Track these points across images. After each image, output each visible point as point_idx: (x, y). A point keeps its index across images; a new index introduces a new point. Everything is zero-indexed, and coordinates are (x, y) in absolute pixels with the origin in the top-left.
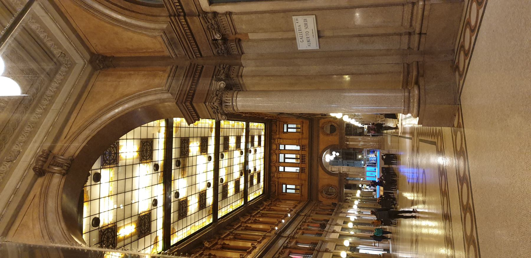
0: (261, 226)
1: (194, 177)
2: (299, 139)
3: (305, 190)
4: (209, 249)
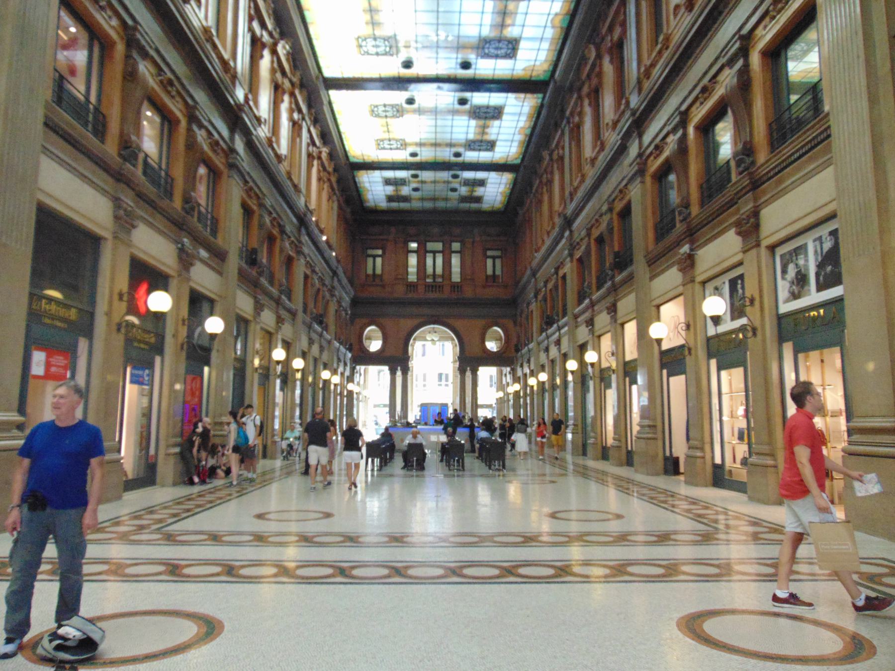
2: (473, 280)
4: (274, 52)
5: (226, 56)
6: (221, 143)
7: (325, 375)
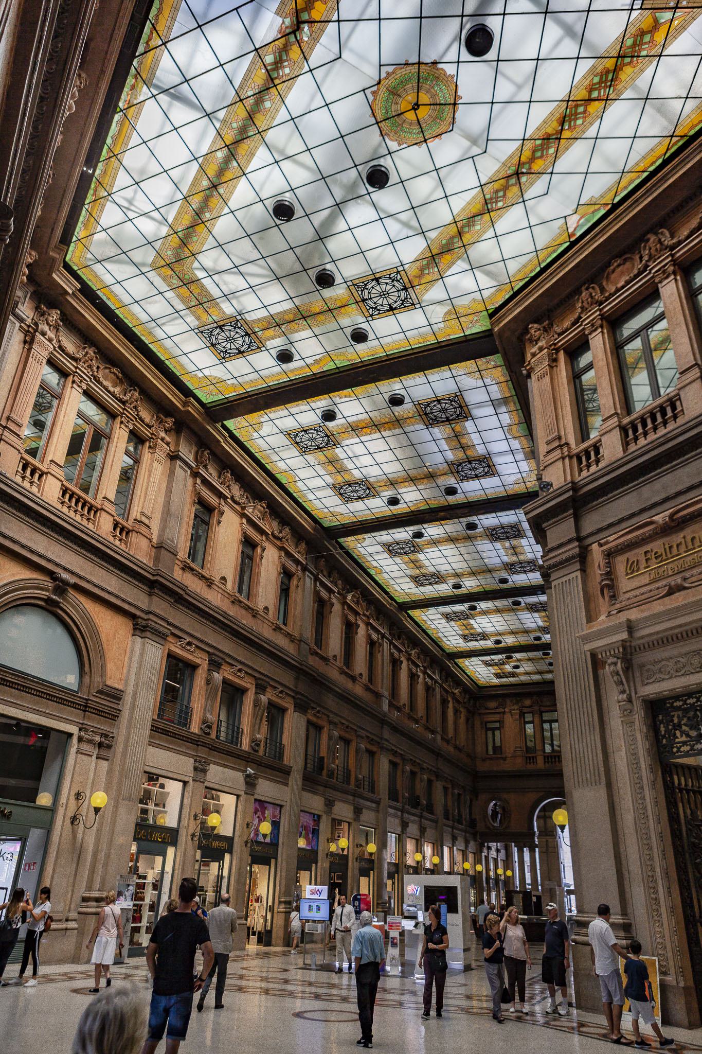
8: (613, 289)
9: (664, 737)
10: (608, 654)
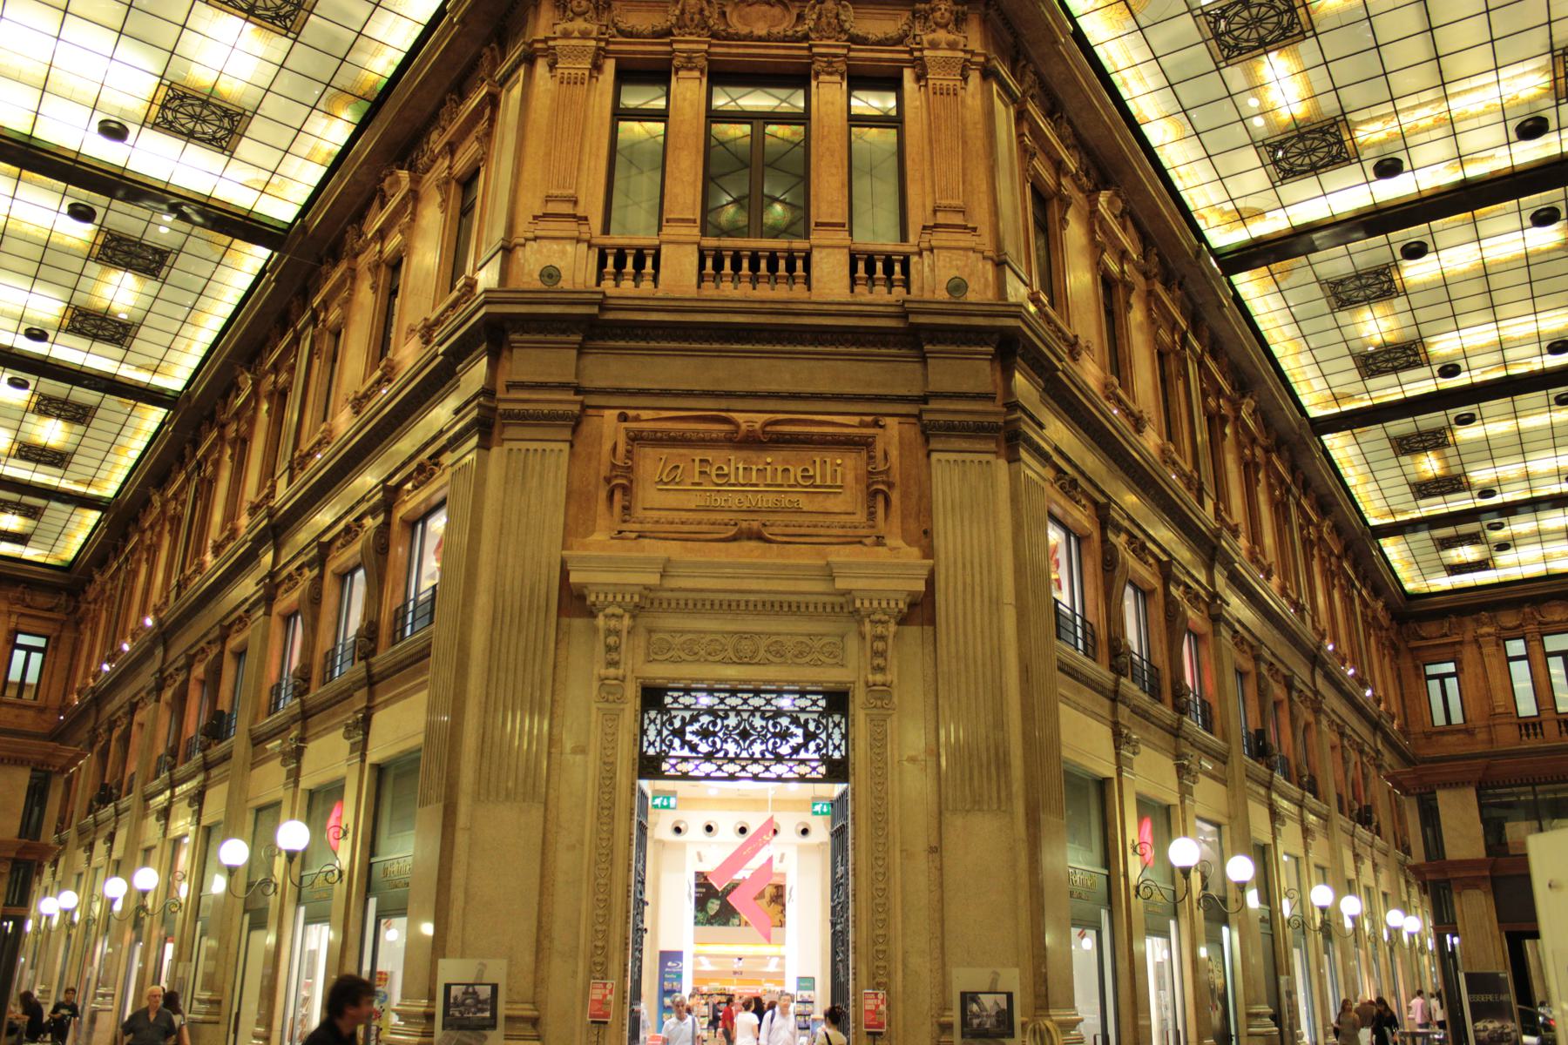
0: (1321, 600)
1: (1482, 301)
3: (1452, 746)
5: (1188, 468)
6: (1202, 593)
7: (1394, 917)
8: (744, 30)
9: (651, 744)
10: (610, 598)
